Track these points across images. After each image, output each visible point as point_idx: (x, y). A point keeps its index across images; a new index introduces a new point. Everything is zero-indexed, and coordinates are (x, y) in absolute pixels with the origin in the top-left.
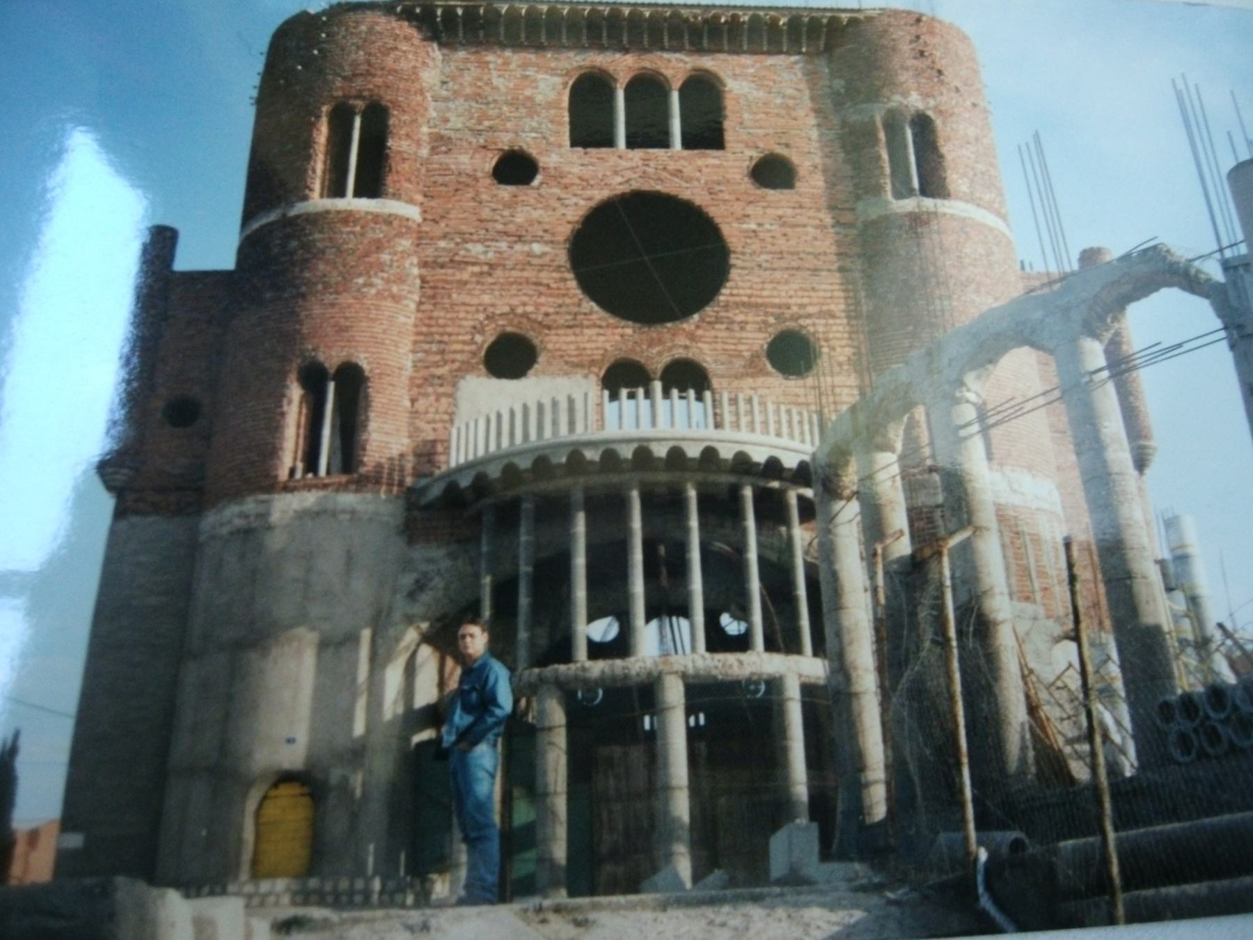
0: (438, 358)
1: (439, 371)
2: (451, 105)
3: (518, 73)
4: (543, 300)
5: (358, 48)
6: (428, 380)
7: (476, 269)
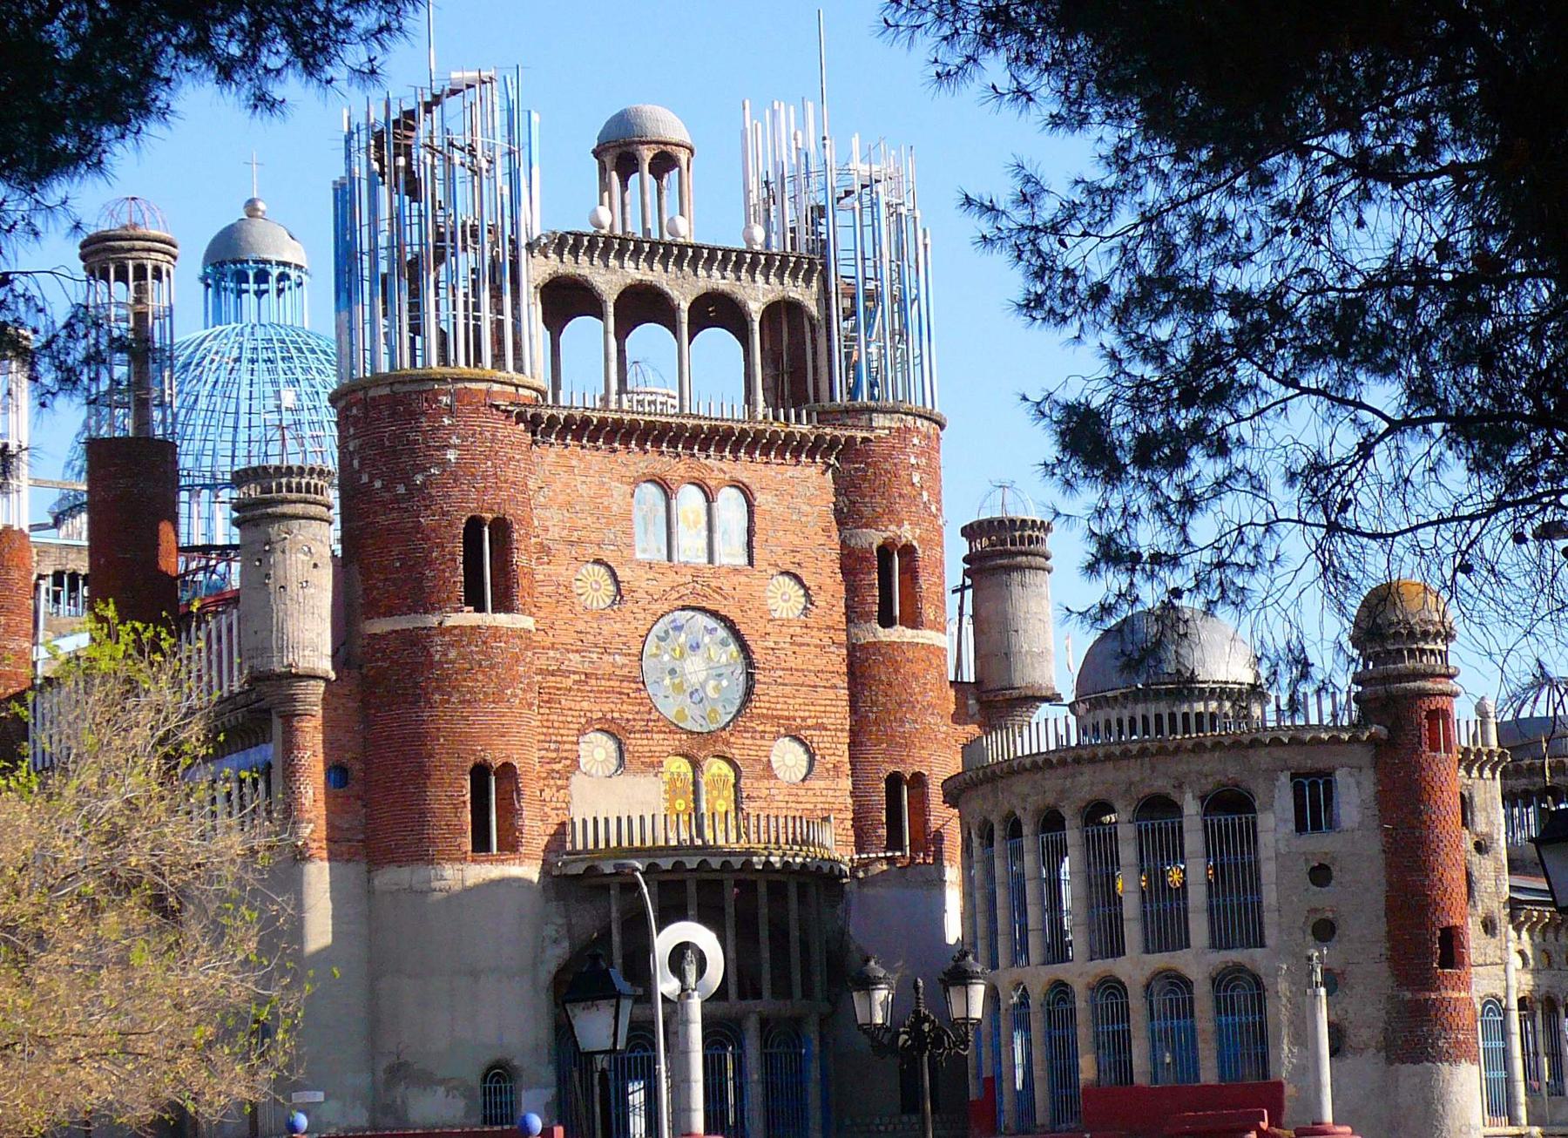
0: (554, 755)
1: (557, 767)
4: (625, 707)
5: (487, 458)
7: (577, 677)
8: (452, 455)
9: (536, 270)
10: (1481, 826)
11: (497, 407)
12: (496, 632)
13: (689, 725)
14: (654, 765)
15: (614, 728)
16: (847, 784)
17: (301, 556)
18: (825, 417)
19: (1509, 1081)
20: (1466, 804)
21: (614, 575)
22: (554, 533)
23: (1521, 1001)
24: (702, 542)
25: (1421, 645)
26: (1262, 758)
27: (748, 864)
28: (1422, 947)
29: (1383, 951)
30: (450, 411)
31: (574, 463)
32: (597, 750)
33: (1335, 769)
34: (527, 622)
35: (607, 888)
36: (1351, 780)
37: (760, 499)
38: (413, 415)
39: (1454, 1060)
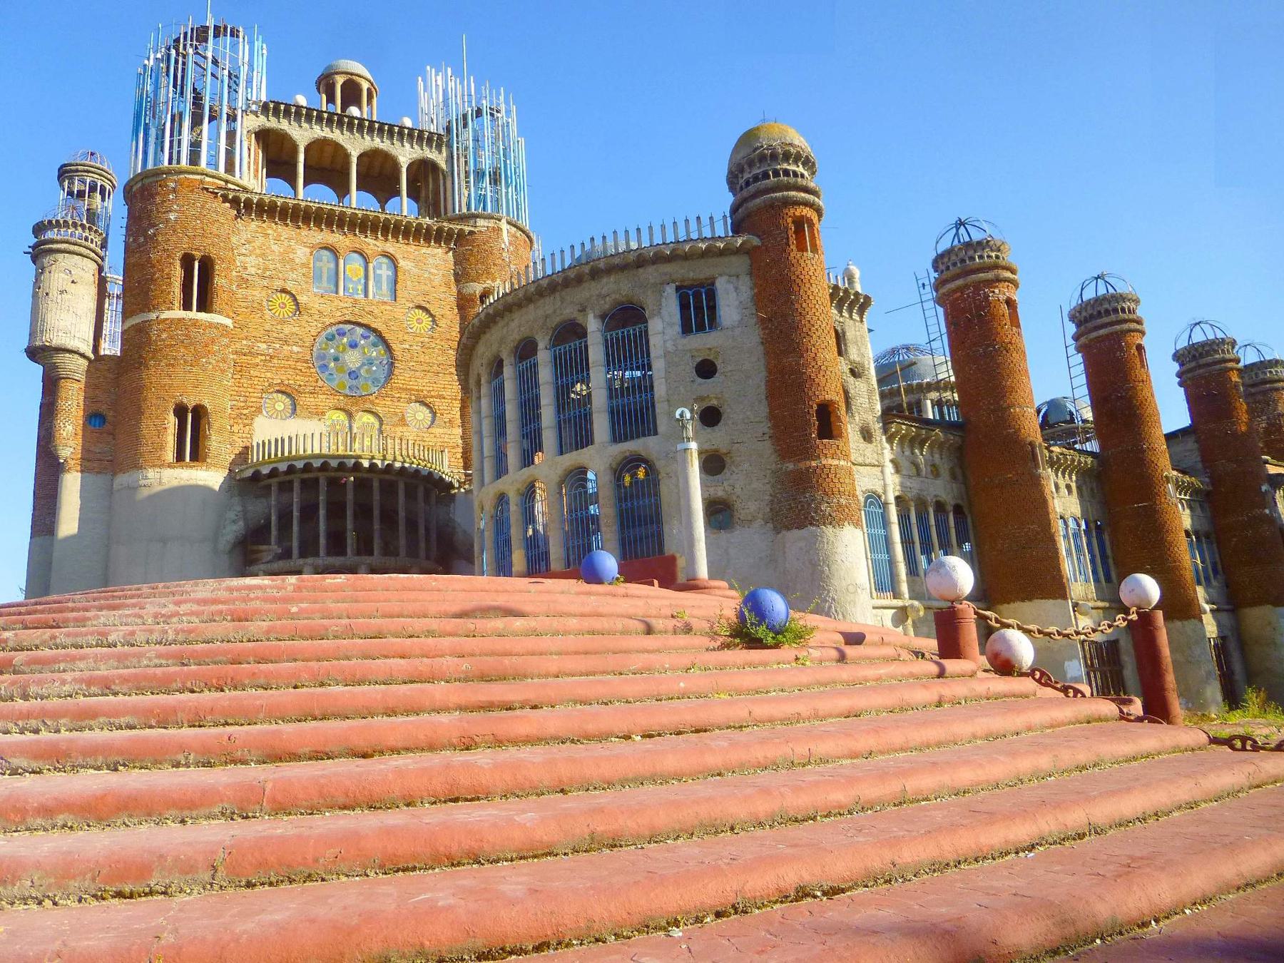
1: (245, 412)
2: (248, 259)
3: (286, 243)
6: (239, 416)
8: (172, 216)
9: (249, 123)
10: (853, 353)
11: (207, 189)
12: (195, 323)
13: (347, 392)
14: (320, 414)
15: (288, 390)
16: (459, 431)
17: (62, 275)
18: (450, 220)
19: (892, 563)
20: (840, 338)
21: (295, 299)
22: (253, 271)
23: (897, 498)
24: (360, 287)
25: (785, 166)
26: (651, 274)
27: (357, 466)
28: (802, 422)
29: (766, 430)
30: (174, 190)
31: (270, 232)
32: (282, 403)
33: (715, 278)
34: (229, 322)
35: (269, 487)
36: (731, 287)
37: (402, 263)
38: (152, 196)
39: (835, 522)
